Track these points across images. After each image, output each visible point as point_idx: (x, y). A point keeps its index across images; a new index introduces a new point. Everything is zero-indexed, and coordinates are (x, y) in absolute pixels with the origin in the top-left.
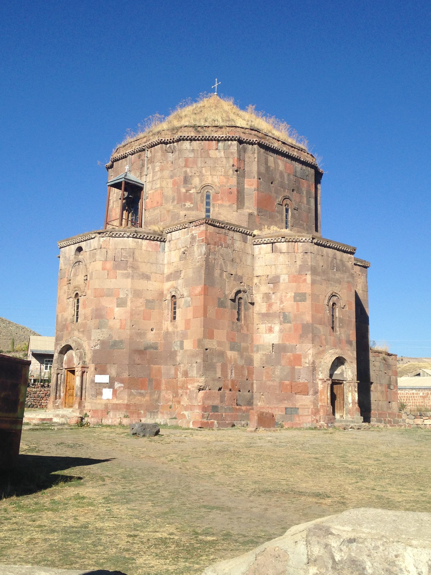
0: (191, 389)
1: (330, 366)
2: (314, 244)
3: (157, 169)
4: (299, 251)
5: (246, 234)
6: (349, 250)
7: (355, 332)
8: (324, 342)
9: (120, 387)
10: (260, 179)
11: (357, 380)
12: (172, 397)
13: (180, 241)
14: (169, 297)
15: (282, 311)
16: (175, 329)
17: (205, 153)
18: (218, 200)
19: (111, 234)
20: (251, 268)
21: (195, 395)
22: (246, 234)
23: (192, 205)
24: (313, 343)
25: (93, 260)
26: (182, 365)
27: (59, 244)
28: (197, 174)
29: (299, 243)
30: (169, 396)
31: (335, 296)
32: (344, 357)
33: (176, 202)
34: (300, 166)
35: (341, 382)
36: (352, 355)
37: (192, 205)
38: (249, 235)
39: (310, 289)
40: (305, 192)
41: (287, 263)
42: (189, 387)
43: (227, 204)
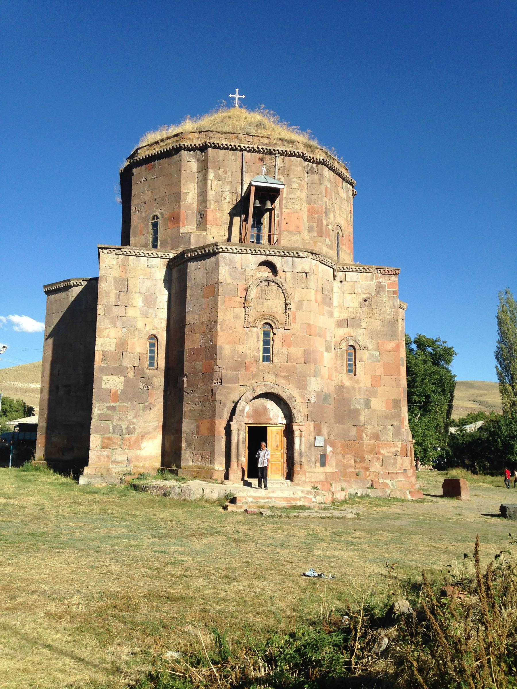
0: (386, 454)
3: (295, 186)
9: (330, 452)
12: (353, 462)
13: (360, 285)
14: (344, 345)
16: (356, 385)
19: (322, 258)
21: (392, 461)
23: (330, 243)
25: (303, 285)
26: (369, 426)
27: (224, 247)
30: (350, 460)
33: (315, 234)
37: (330, 243)
42: (382, 451)
43: (348, 251)
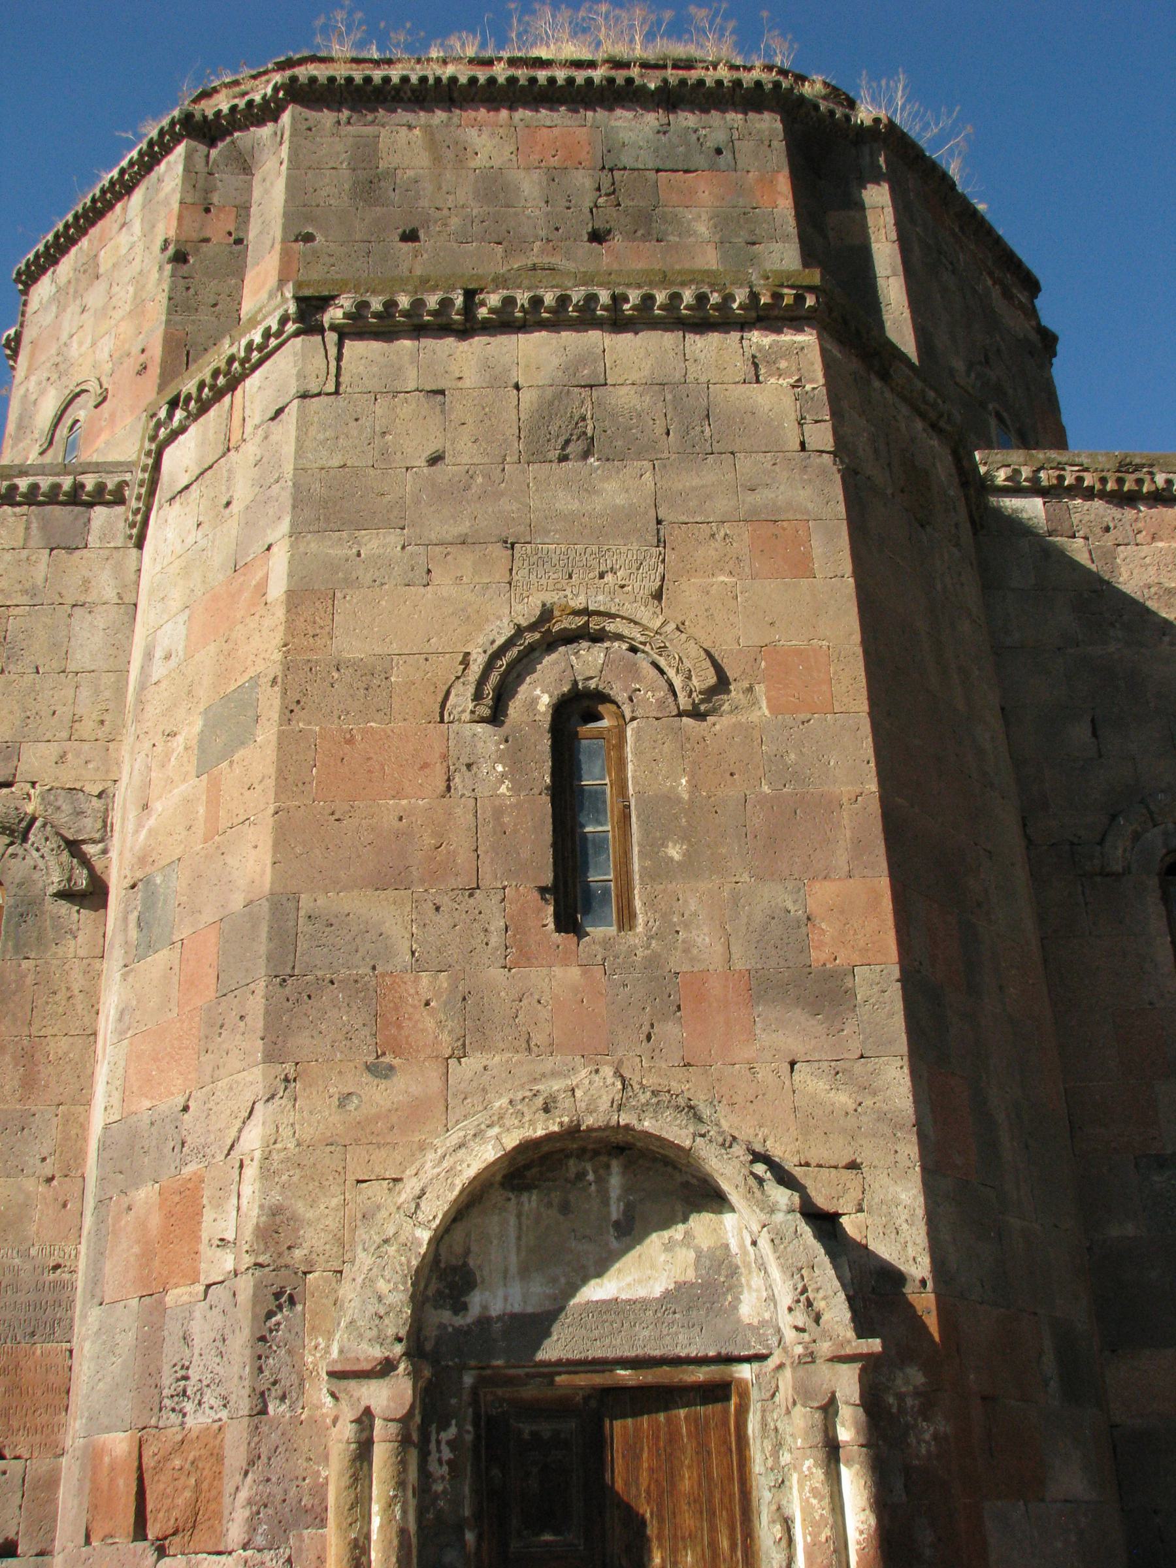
1: (425, 1235)
2: (331, 337)
4: (249, 429)
5: (75, 498)
6: (735, 306)
7: (884, 884)
8: (430, 1023)
10: (308, 238)
11: (863, 1328)
15: (139, 875)
17: (91, 272)
18: (101, 430)
20: (108, 679)
22: (75, 498)
24: (272, 1056)
28: (54, 377)
29: (248, 382)
31: (598, 638)
32: (647, 1125)
34: (652, 119)
35: (700, 1375)
36: (843, 1099)
38: (100, 497)
39: (278, 637)
40: (703, 229)
41: (190, 540)
